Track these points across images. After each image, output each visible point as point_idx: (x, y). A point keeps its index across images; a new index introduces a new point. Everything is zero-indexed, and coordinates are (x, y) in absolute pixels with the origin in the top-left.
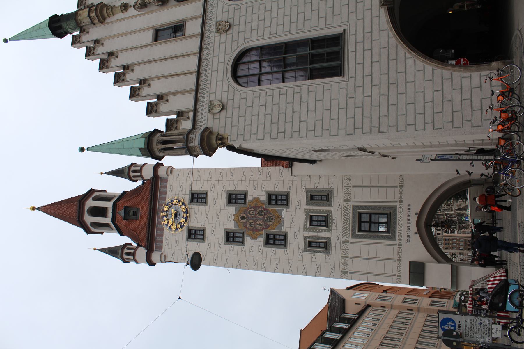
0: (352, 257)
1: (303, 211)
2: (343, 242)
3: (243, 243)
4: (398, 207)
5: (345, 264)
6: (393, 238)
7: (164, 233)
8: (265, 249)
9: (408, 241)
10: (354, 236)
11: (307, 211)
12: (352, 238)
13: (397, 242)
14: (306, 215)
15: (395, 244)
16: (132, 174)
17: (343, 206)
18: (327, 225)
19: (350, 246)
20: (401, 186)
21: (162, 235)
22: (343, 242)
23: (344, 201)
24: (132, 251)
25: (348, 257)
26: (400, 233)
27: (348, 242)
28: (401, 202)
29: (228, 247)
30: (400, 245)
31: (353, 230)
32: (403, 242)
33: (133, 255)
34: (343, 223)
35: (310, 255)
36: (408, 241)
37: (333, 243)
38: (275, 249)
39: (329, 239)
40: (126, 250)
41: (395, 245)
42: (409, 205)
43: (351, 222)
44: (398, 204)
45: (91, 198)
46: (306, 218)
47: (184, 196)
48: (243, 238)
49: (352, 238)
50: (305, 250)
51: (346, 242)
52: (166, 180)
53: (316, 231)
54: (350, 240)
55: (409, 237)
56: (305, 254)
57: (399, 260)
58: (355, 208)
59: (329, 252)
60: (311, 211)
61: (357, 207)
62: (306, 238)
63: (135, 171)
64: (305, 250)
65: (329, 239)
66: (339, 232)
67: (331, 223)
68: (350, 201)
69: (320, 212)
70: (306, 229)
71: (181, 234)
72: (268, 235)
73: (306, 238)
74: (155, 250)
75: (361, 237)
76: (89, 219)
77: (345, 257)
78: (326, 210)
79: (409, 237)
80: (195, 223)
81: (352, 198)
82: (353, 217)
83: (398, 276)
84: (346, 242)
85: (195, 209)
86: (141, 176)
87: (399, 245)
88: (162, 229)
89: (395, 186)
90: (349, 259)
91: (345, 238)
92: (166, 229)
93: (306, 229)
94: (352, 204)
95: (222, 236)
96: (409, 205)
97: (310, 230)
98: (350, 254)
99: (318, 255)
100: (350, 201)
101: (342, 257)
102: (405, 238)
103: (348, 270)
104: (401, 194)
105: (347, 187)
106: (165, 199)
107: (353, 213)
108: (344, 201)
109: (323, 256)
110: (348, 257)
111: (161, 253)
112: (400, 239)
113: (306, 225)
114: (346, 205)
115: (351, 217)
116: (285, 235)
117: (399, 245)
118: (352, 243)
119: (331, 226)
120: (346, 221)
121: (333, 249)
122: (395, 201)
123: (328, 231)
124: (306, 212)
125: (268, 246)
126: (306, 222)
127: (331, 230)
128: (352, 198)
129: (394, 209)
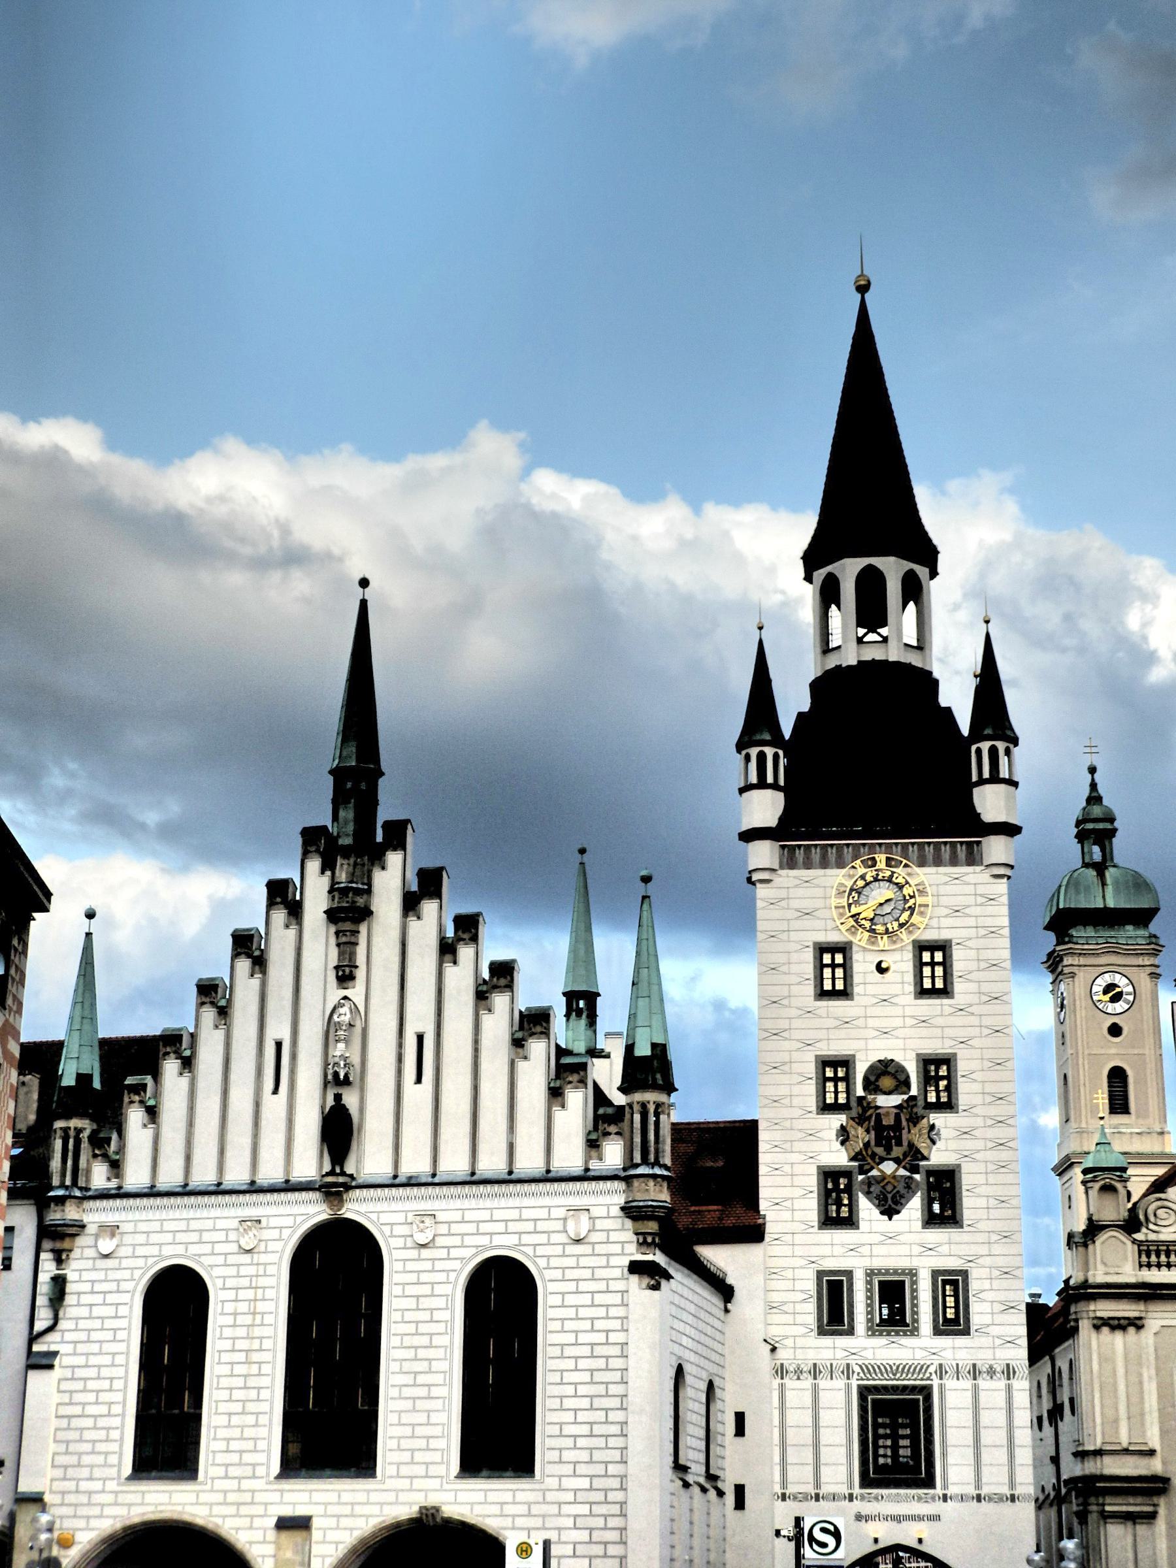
0: (815, 1390)
1: (914, 1263)
2: (848, 1365)
3: (826, 1108)
4: (931, 1491)
5: (799, 1373)
6: (866, 1482)
7: (829, 871)
8: (814, 1171)
9: (859, 1517)
10: (864, 1392)
11: (913, 1273)
12: (859, 1386)
13: (857, 1490)
14: (903, 1272)
15: (851, 1486)
16: (985, 746)
17: (928, 1363)
18: (883, 1322)
19: (840, 1383)
20: (979, 1498)
21: (824, 865)
22: (848, 1365)
23: (941, 1365)
24: (770, 779)
25: (815, 1378)
26: (876, 1498)
27: (848, 1378)
28: (945, 1498)
29: (811, 1069)
30: (851, 1498)
31: (876, 1389)
32: (858, 1506)
33: (762, 784)
34: (891, 1363)
35: (811, 1286)
36: (859, 1517)
37: (842, 1341)
38: (815, 1195)
39: (851, 1332)
40: (769, 751)
41: (851, 1486)
42: (936, 1518)
43: (895, 1382)
44: (939, 1491)
45: (908, 565)
46: (896, 1272)
47: (934, 923)
48: (835, 1108)
49: (859, 1386)
50: (820, 1274)
51: (848, 1371)
52: (973, 859)
53: (868, 1298)
54: (854, 1383)
55: (867, 1518)
56: (811, 1275)
57: (817, 1498)
58: (926, 1391)
59: (822, 1332)
60: (914, 1283)
61: (928, 1398)
62: (849, 1274)
63: (993, 752)
64: (820, 1274)
65: (851, 1332)
66: (868, 1354)
67: (889, 1334)
68: (941, 1378)
69: (915, 1306)
70: (870, 1274)
71: (830, 924)
72: (847, 1174)
73: (849, 1274)
74: (783, 847)
75: (863, 1409)
76: (849, 570)
77: (815, 1372)
78: (917, 1321)
79: (867, 1518)
80: (863, 964)
81: (950, 1383)
82: (905, 1388)
83: (784, 1495)
84: (848, 1371)
85: (902, 962)
86: (982, 782)
87: (851, 1495)
88: (841, 865)
89: (978, 1486)
90: (810, 1380)
91: (857, 1369)
92: (839, 877)
93: (870, 1274)
94: (936, 1383)
95: (836, 1048)
96: (936, 1518)
97: (869, 1283)
98: (823, 1383)
99: (811, 1307)
100: (941, 1378)
101: (815, 1365)
102: (867, 1508)
103: (786, 1381)
104: (962, 1498)
105: (975, 1372)
106: (922, 864)
107: (913, 1389)
108: (941, 1365)
109: (812, 1320)
110: (815, 1378)
111: (776, 866)
112: (863, 1498)
113: (880, 1272)
114: (932, 1369)
115: (906, 1382)
116: (850, 1222)
117: (851, 1495)
118: (848, 1386)
119: (881, 1335)
120: (896, 1370)
121: (828, 1341)
122: (945, 1487)
123: (869, 1329)
124: (911, 1270)
125: (822, 1177)
126: (887, 1271)
127: (873, 1335)
128: (950, 1383)
129: (929, 1482)
